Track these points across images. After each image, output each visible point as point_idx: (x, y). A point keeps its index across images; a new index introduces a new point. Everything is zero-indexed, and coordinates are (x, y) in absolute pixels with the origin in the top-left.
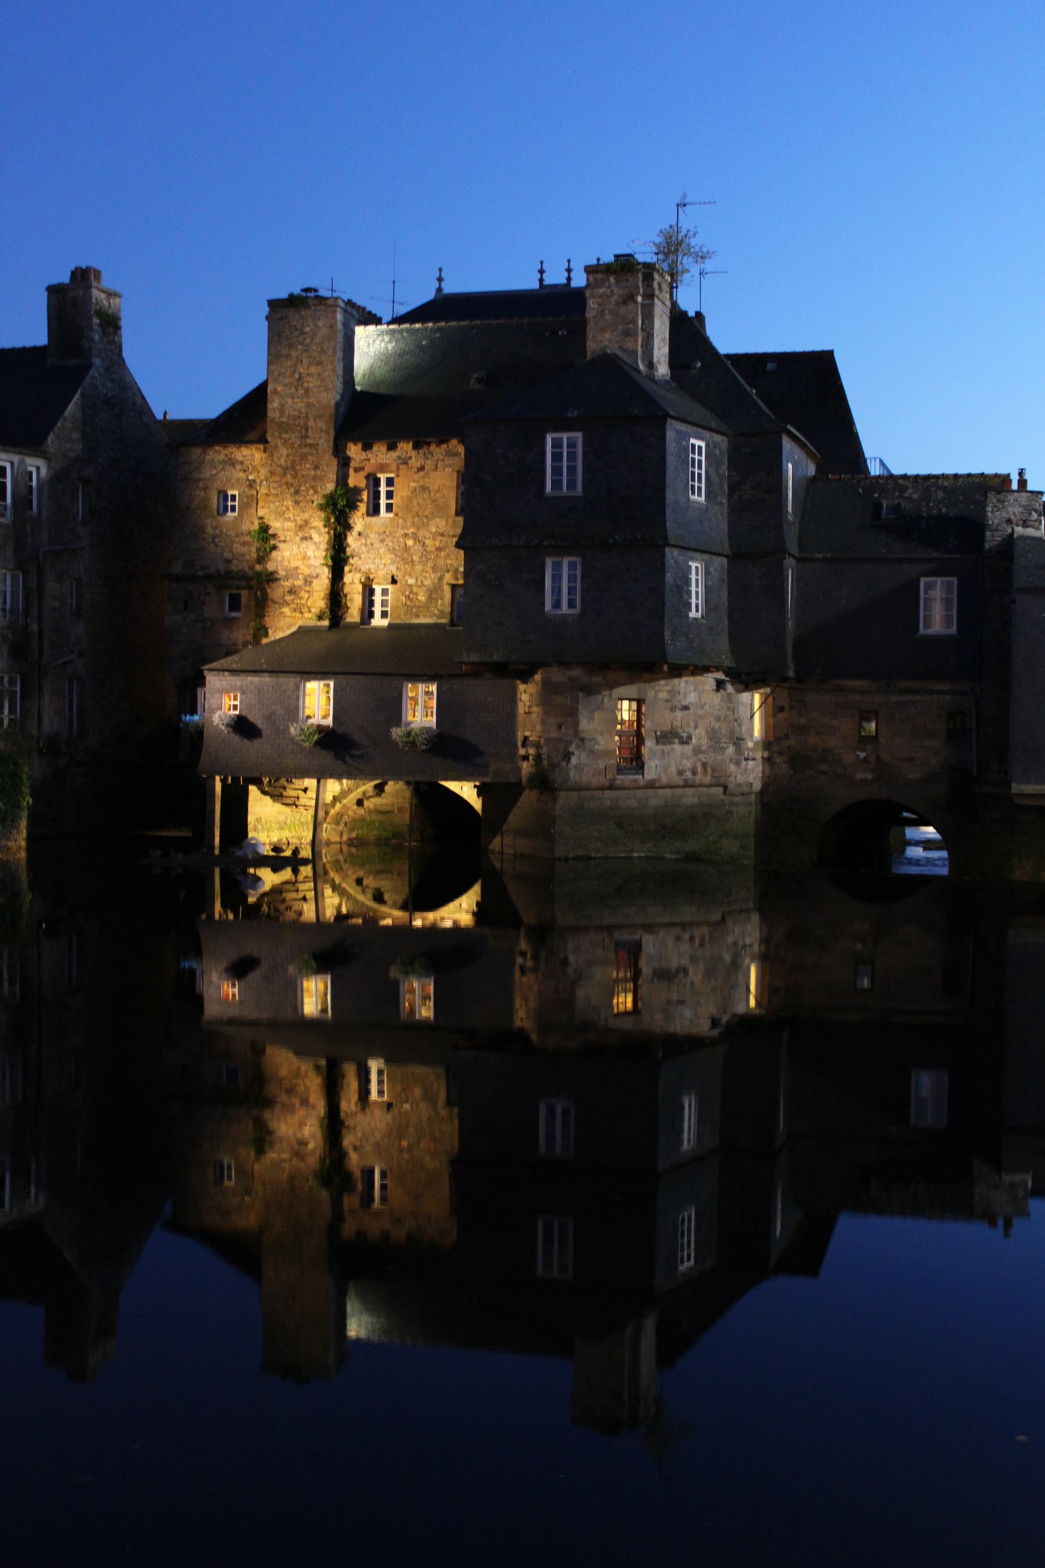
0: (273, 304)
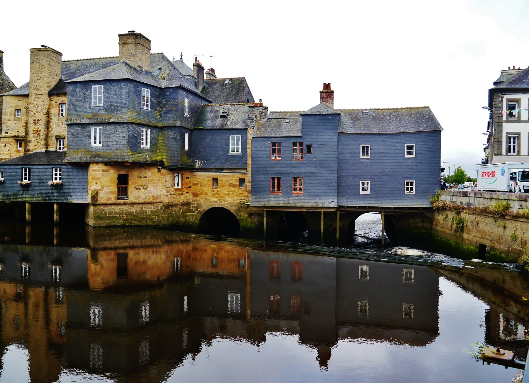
0: (32, 51)
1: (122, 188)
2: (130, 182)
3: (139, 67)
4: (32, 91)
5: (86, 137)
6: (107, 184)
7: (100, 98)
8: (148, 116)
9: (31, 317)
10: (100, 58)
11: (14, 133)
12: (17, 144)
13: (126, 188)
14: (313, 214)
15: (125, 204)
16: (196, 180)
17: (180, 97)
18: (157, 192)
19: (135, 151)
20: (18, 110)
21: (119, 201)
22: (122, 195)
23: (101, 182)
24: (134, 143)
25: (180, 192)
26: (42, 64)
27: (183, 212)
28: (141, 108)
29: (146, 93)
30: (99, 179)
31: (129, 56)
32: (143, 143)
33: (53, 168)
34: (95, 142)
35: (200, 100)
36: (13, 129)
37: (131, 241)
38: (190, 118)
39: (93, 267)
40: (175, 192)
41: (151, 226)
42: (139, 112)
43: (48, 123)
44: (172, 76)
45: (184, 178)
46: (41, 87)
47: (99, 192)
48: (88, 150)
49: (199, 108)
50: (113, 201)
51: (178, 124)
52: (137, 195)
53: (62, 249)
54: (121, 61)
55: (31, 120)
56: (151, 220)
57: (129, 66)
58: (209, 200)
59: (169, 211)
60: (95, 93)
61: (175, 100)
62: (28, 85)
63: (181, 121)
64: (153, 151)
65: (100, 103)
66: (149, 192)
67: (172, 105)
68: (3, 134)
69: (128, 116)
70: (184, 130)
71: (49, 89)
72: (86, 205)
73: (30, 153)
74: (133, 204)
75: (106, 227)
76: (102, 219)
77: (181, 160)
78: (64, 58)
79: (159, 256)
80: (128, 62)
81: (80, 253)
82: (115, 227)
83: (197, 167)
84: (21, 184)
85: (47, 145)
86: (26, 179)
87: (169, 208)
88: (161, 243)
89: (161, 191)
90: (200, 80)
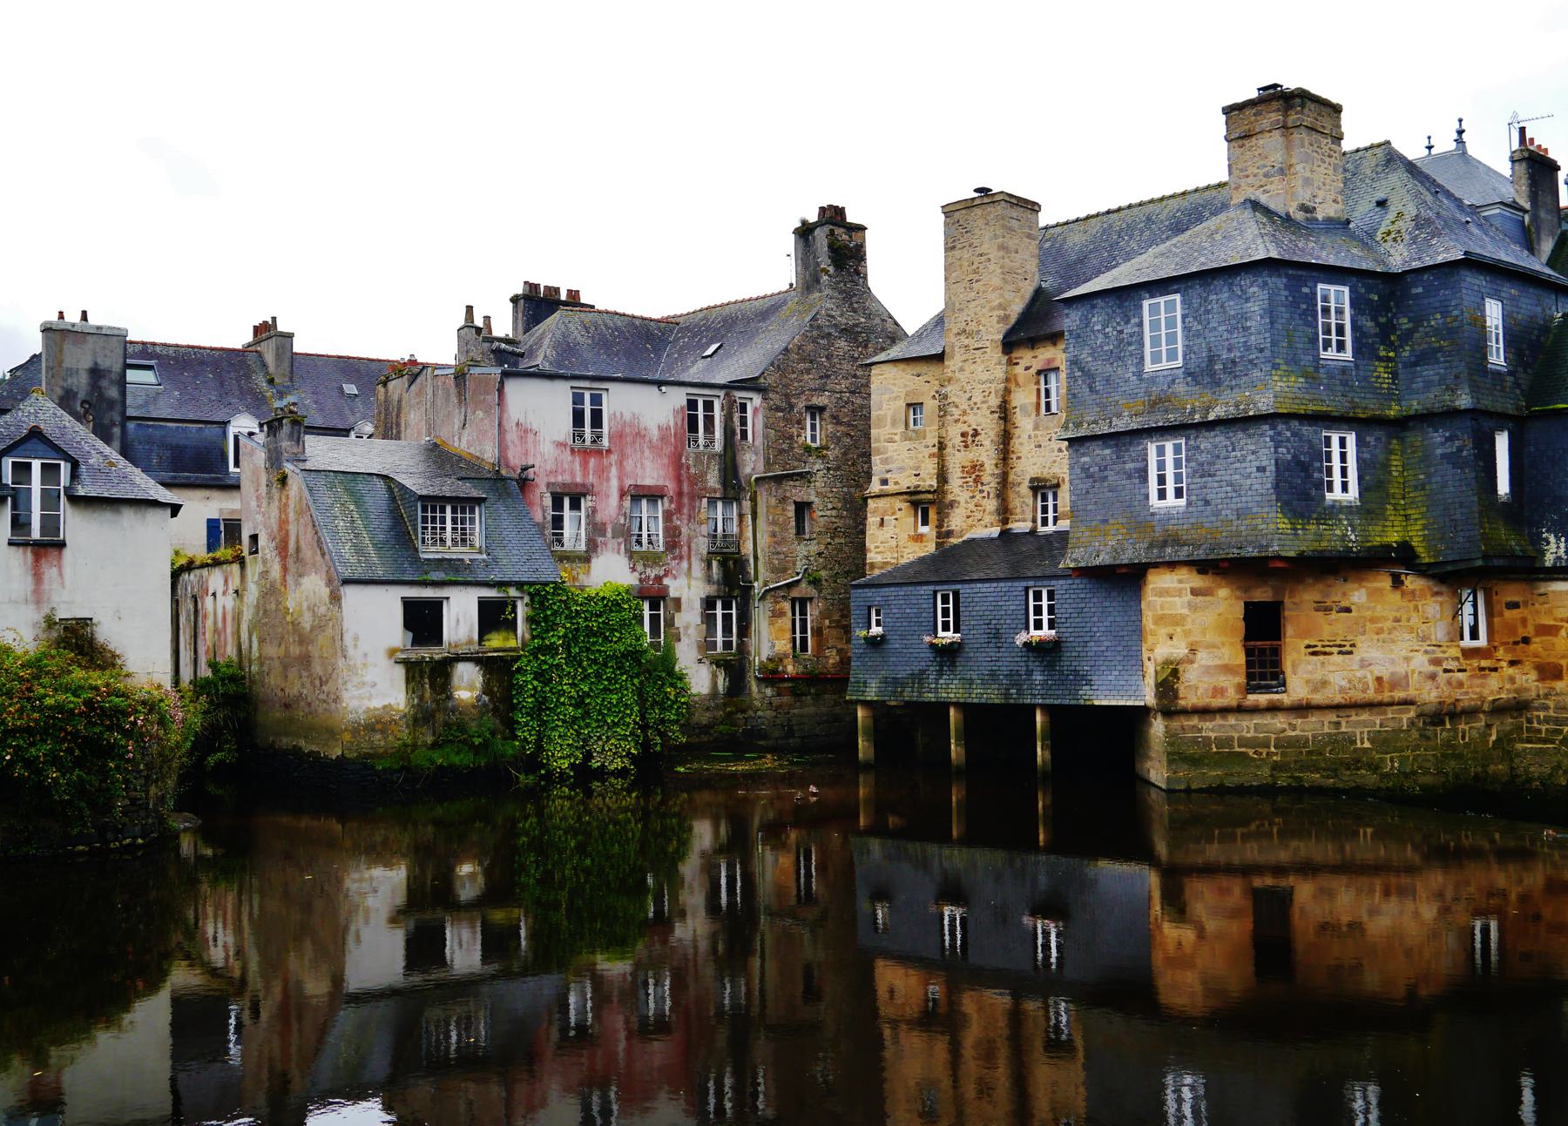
0: (949, 211)
1: (1262, 651)
2: (1289, 630)
3: (1304, 208)
4: (953, 339)
5: (1130, 477)
6: (1210, 637)
7: (1171, 339)
8: (1344, 383)
9: (970, 1091)
10: (1162, 199)
11: (906, 482)
12: (916, 516)
13: (1277, 652)
15: (1273, 709)
16: (1549, 612)
17: (1468, 298)
18: (1393, 662)
19: (1302, 517)
20: (914, 406)
21: (1252, 698)
22: (1263, 677)
23: (1185, 634)
24: (1299, 486)
25: (1484, 663)
26: (979, 251)
27: (1499, 740)
28: (1317, 358)
29: (1337, 296)
30: (1178, 621)
31: (1266, 175)
32: (1330, 484)
33: (1027, 589)
34: (1162, 495)
35: (1549, 299)
36: (902, 469)
37: (1302, 845)
38: (1510, 373)
39: (1172, 933)
40: (1464, 663)
41: (1375, 792)
42: (1314, 372)
43: (1006, 438)
44: (1428, 221)
45: (1497, 608)
46: (979, 323)
47: (1181, 668)
48: (1140, 521)
49: (1545, 329)
50: (1231, 698)
51: (1464, 401)
52: (1318, 676)
53: (1064, 862)
54: (1238, 198)
55: (954, 434)
56: (1375, 767)
57: (1267, 211)
59: (1442, 734)
60: (1155, 325)
61: (1445, 314)
62: (939, 321)
63: (1475, 390)
64: (1369, 512)
65: (1172, 355)
66: (1364, 664)
67: (1437, 331)
68: (875, 487)
69: (1269, 391)
70: (1487, 424)
71: (1004, 328)
72: (1139, 715)
73: (954, 541)
74: (1302, 709)
75: (1209, 791)
76: (1194, 761)
77: (1485, 538)
78: (1045, 219)
79: (1409, 906)
80: (1263, 199)
81: (1124, 879)
82: (1241, 791)
83: (1549, 560)
84: (932, 645)
85: (1004, 513)
86: (946, 627)
87: (1442, 723)
88: (1417, 859)
89: (1407, 659)
90: (1542, 214)
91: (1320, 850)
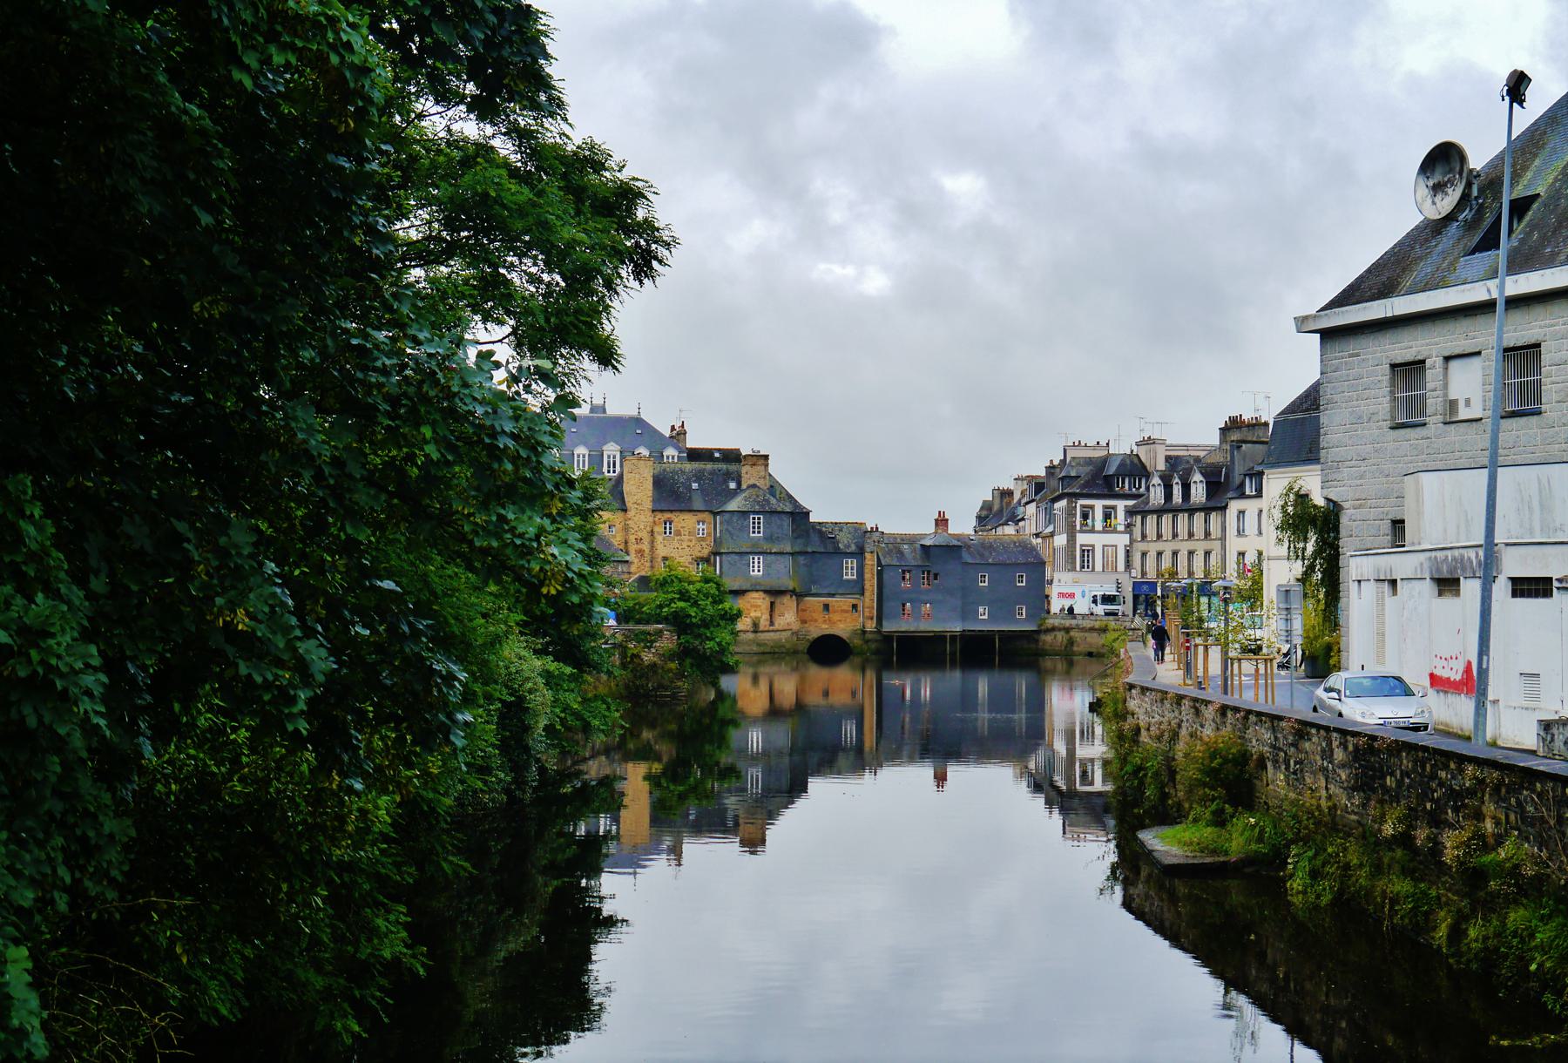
14: (938, 639)
43: (652, 542)
48: (748, 577)
55: (632, 538)
58: (820, 627)
91: (775, 669)
